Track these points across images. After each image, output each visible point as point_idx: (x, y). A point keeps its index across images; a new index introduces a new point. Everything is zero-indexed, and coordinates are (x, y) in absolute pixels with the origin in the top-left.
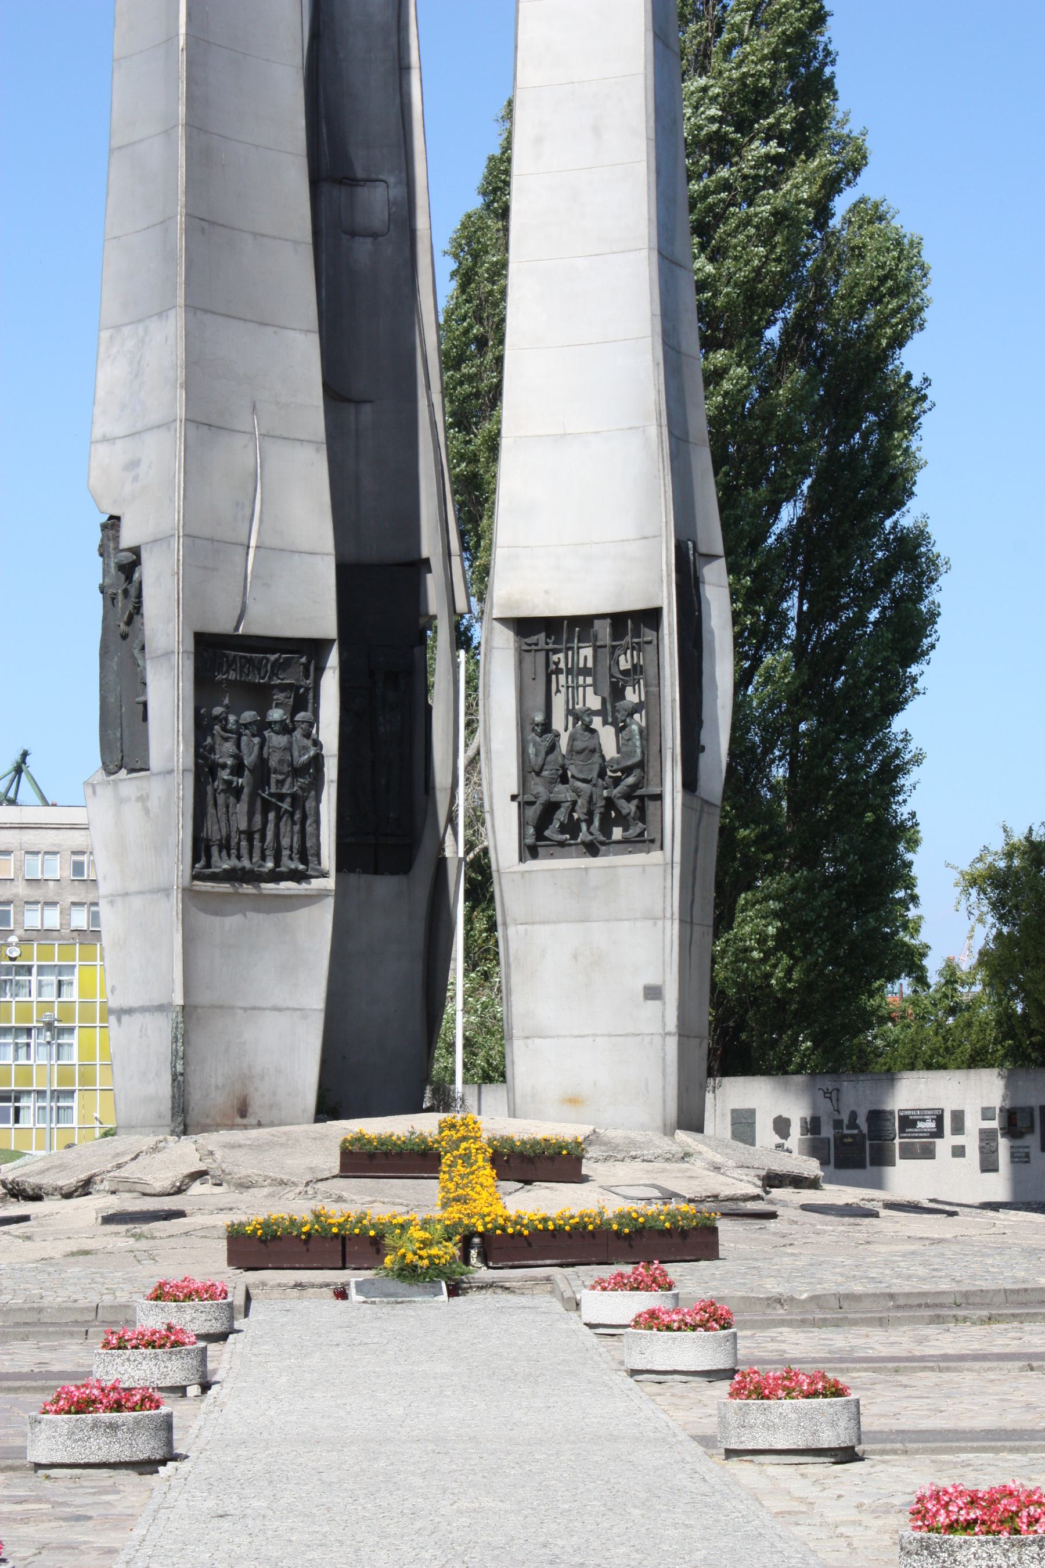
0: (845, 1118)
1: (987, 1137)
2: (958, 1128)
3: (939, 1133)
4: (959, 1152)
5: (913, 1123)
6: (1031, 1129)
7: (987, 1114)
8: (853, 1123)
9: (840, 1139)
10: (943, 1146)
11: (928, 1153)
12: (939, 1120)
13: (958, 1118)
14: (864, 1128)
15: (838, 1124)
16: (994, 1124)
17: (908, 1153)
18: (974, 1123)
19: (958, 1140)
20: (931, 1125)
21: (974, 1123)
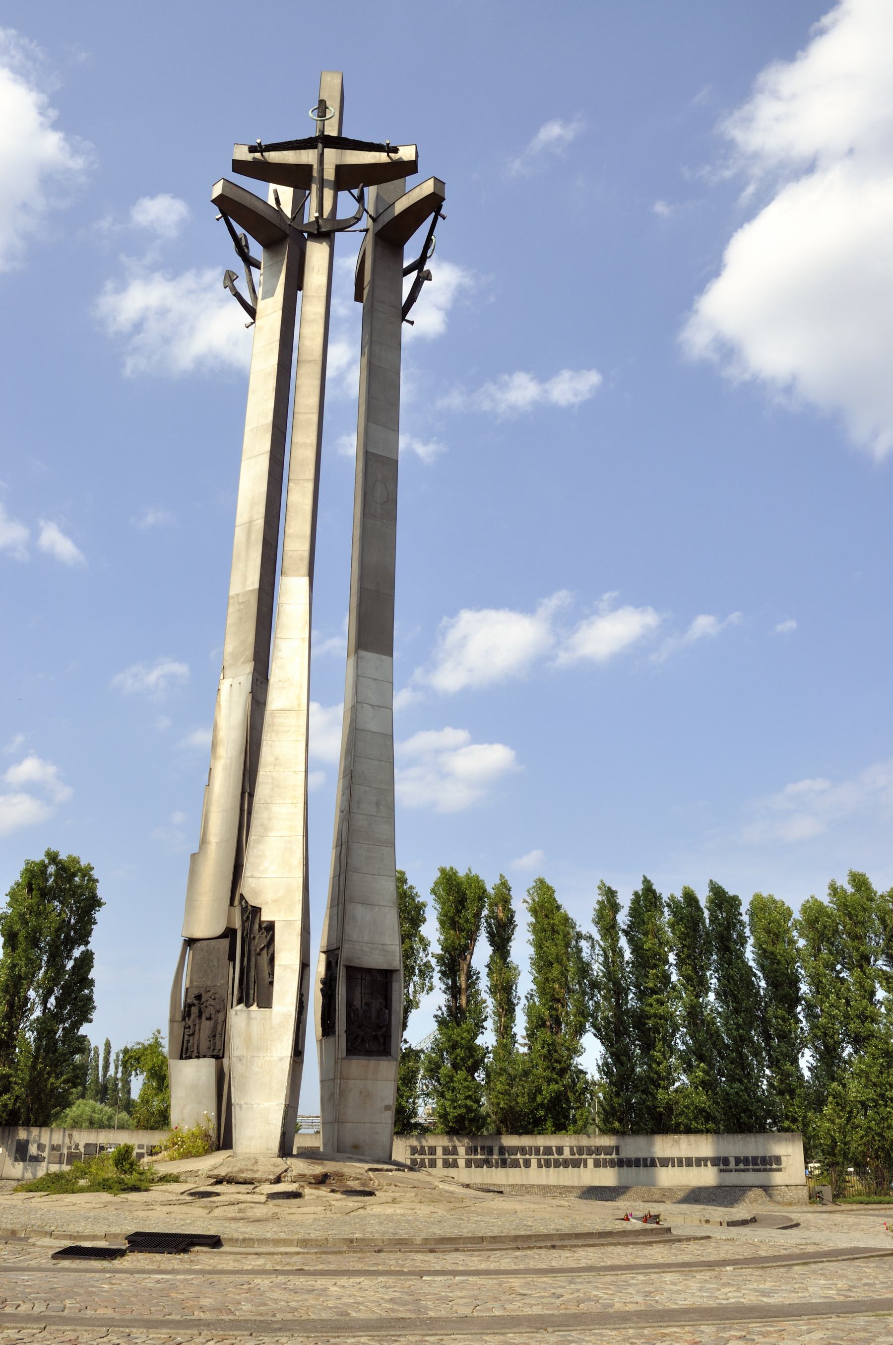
14: (82, 1150)
15: (69, 1148)
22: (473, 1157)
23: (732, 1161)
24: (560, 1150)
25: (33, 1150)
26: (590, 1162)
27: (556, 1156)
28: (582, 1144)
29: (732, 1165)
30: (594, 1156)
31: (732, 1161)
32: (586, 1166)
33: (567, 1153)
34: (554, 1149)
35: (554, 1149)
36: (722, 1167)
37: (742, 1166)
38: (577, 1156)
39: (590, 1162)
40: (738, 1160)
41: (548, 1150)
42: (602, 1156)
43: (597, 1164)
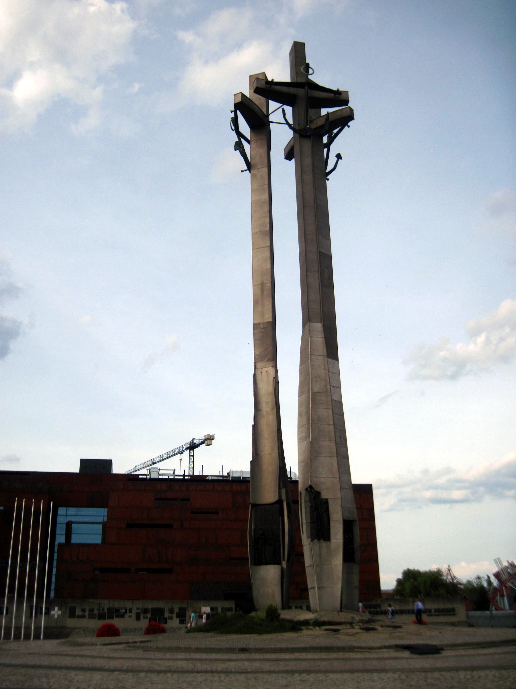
0: (101, 609)
3: (126, 612)
4: (130, 617)
5: (119, 610)
6: (148, 612)
7: (138, 609)
8: (103, 610)
10: (127, 616)
12: (126, 610)
13: (131, 611)
14: (106, 611)
15: (99, 610)
16: (140, 611)
17: (117, 616)
18: (134, 611)
19: (130, 614)
20: (123, 611)
21: (134, 611)
23: (433, 610)
25: (78, 612)
29: (433, 613)
31: (433, 610)
36: (428, 614)
37: (437, 613)
40: (436, 610)
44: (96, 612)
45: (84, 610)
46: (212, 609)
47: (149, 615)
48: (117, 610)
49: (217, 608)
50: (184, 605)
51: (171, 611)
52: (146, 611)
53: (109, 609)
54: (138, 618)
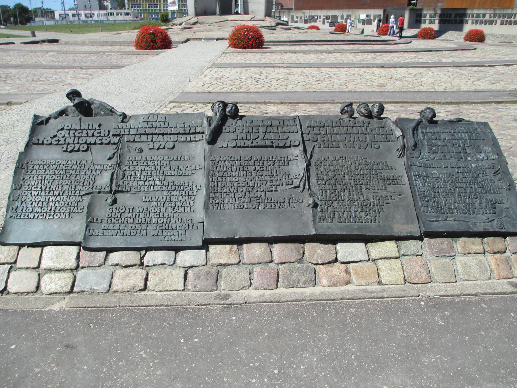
1: (324, 20)
2: (320, 18)
3: (317, 19)
4: (320, 21)
7: (324, 16)
9: (305, 20)
10: (318, 21)
11: (316, 22)
13: (320, 17)
17: (314, 22)
21: (322, 18)
22: (442, 19)
24: (484, 16)
25: (295, 19)
26: (499, 22)
27: (481, 19)
28: (474, 13)
30: (501, 19)
32: (496, 24)
33: (487, 17)
34: (481, 15)
35: (481, 15)
38: (492, 19)
39: (499, 22)
41: (478, 16)
42: (506, 19)
43: (502, 23)
44: (303, 18)
45: (297, 17)
46: (367, 16)
47: (330, 21)
48: (313, 17)
49: (371, 15)
50: (350, 13)
51: (342, 17)
52: (327, 18)
53: (309, 16)
54: (324, 23)
